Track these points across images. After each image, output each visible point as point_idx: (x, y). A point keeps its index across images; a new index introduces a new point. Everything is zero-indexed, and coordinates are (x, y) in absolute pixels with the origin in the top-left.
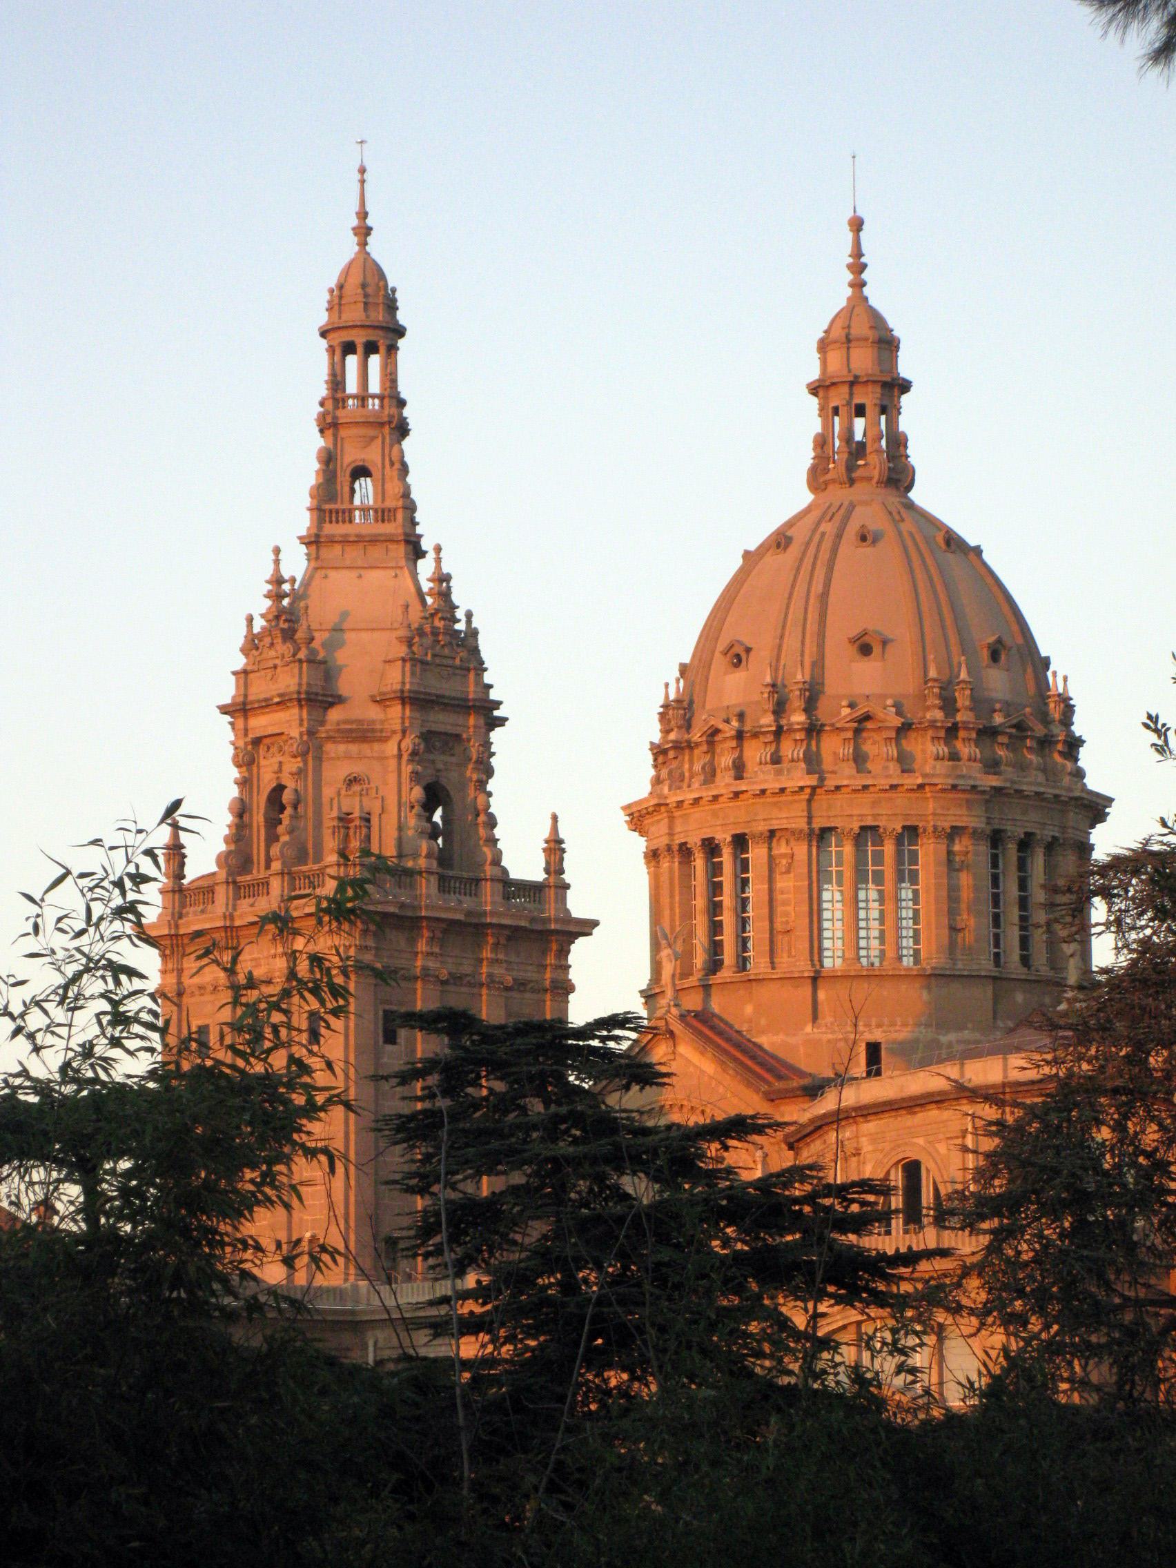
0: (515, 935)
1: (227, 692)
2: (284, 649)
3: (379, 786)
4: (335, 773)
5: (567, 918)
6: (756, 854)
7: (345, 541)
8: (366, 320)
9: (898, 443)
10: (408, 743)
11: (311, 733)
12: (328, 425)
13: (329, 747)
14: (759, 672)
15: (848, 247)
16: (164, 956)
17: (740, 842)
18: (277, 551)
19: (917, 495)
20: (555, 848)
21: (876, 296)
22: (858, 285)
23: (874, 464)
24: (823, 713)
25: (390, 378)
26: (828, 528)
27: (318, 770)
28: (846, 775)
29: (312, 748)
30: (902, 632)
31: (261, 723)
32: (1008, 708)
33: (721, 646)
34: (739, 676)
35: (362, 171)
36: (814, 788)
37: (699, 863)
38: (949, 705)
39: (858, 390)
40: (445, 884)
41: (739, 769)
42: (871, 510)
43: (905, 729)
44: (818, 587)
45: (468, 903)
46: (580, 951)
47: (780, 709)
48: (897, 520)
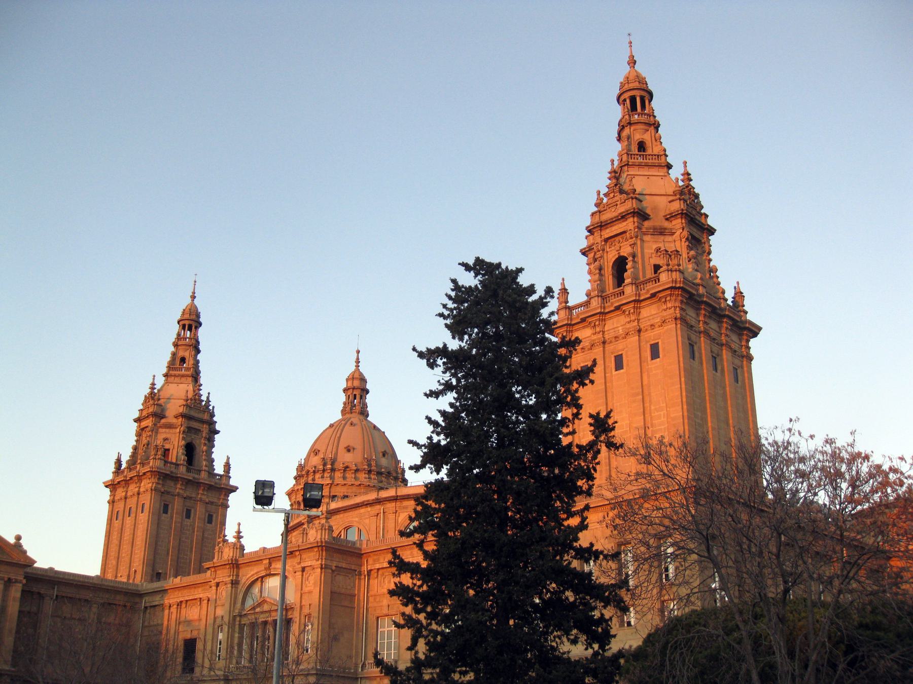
0: (211, 488)
1: (137, 415)
2: (151, 402)
3: (176, 443)
4: (161, 437)
5: (228, 484)
7: (175, 376)
8: (191, 322)
11: (155, 425)
12: (176, 345)
13: (160, 430)
20: (227, 466)
21: (361, 369)
22: (358, 366)
23: (358, 409)
24: (336, 466)
25: (196, 335)
27: (156, 436)
29: (155, 429)
30: (358, 446)
31: (144, 424)
32: (386, 468)
34: (317, 457)
38: (369, 465)
40: (188, 470)
42: (355, 418)
43: (357, 471)
45: (196, 476)
46: (232, 497)
47: (325, 465)
48: (361, 421)
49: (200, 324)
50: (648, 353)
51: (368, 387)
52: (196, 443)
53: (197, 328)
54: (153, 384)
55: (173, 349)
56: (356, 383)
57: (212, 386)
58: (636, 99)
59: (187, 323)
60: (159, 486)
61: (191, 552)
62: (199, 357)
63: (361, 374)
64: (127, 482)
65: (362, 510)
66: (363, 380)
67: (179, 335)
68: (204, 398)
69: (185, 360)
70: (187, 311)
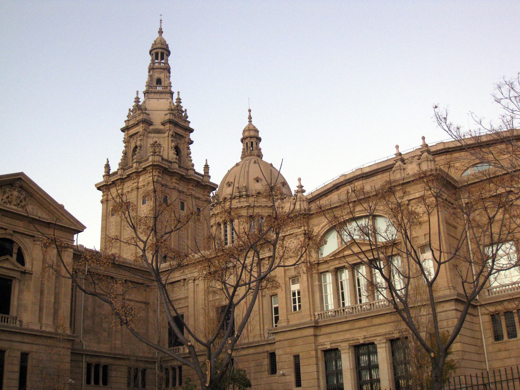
1: (124, 125)
8: (160, 52)
9: (260, 149)
10: (171, 133)
13: (150, 135)
16: (103, 192)
18: (138, 92)
19: (263, 159)
20: (207, 167)
21: (253, 123)
22: (250, 121)
25: (166, 63)
31: (132, 131)
33: (226, 183)
35: (161, 21)
37: (222, 226)
44: (246, 170)
49: (169, 53)
51: (260, 135)
52: (181, 147)
56: (252, 133)
59: (160, 51)
60: (160, 179)
61: (188, 239)
63: (254, 127)
64: (122, 180)
66: (257, 131)
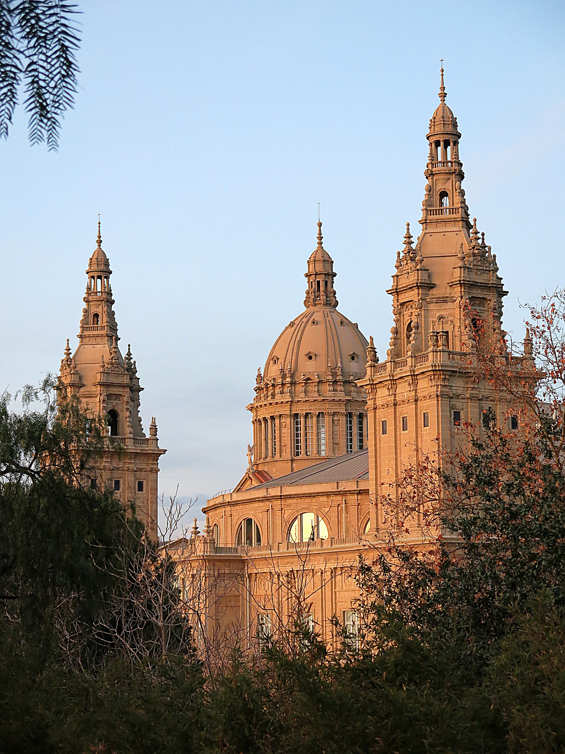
6: (277, 421)
14: (279, 366)
15: (317, 232)
17: (273, 418)
20: (154, 428)
26: (304, 320)
28: (302, 396)
30: (322, 352)
34: (276, 366)
36: (292, 401)
39: (317, 276)
41: (273, 395)
47: (284, 377)
50: (421, 421)
52: (118, 409)
53: (107, 278)
54: (68, 349)
55: (85, 305)
57: (132, 337)
58: (446, 134)
62: (114, 308)
65: (256, 505)
67: (89, 288)
68: (124, 355)
69: (100, 316)
70: (94, 260)
